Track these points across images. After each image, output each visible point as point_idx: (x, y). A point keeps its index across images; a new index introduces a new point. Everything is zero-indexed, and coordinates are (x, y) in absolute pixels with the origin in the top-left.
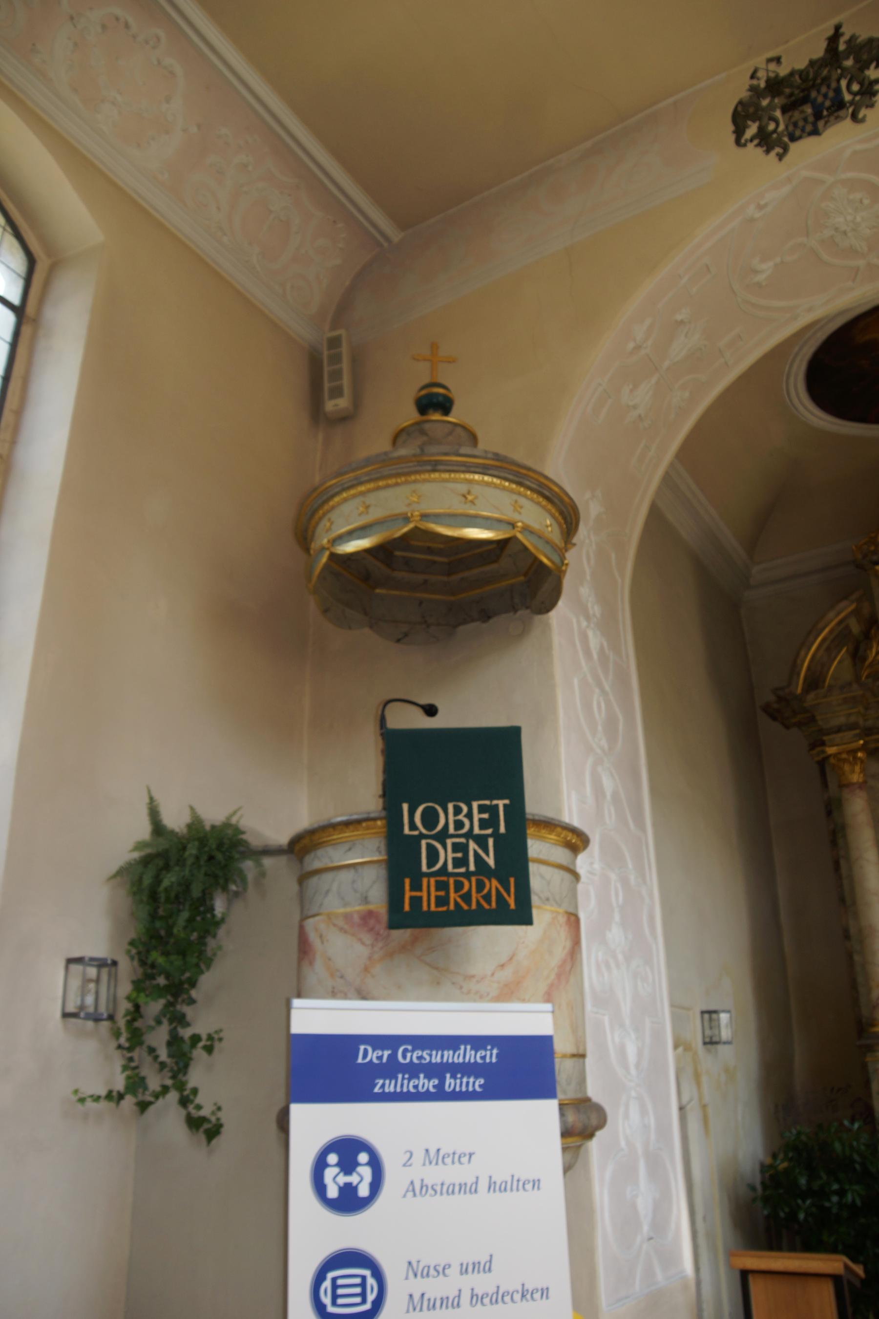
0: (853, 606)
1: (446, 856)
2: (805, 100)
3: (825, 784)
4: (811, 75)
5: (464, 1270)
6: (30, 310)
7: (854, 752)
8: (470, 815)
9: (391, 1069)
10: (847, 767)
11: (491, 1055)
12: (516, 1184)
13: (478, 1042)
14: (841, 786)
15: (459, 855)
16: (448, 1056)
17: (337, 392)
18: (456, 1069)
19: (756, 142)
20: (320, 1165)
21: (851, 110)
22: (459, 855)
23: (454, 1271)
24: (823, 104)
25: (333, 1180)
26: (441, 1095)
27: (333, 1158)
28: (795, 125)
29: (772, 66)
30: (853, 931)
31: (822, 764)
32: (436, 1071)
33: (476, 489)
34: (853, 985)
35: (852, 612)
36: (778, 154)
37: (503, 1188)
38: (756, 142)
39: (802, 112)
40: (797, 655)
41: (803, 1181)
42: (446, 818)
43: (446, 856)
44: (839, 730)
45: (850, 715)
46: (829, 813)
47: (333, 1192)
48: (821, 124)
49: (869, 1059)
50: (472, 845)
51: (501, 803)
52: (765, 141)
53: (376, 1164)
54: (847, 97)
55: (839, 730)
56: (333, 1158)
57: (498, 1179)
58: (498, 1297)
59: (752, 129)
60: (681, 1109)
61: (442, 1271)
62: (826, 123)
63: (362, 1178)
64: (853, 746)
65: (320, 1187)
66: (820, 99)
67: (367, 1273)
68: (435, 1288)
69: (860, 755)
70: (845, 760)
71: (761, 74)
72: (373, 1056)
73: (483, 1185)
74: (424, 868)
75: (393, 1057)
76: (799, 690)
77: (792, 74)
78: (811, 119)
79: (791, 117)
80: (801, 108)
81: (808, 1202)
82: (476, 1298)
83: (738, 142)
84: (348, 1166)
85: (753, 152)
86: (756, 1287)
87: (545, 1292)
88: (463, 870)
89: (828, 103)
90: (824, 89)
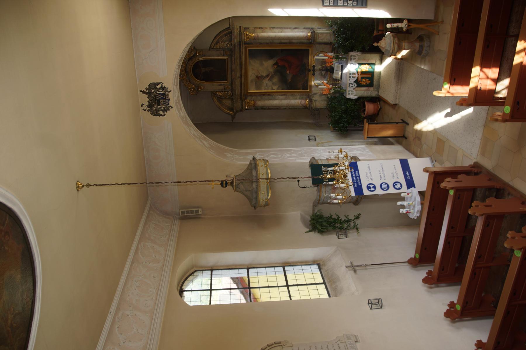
2: (159, 101)
3: (250, 109)
4: (152, 98)
5: (380, 173)
6: (210, 269)
8: (325, 172)
10: (251, 104)
11: (353, 170)
12: (369, 167)
15: (331, 173)
16: (354, 176)
17: (197, 211)
18: (356, 175)
19: (165, 112)
20: (371, 191)
21: (166, 92)
22: (331, 173)
23: (380, 174)
24: (161, 97)
25: (372, 189)
26: (359, 176)
27: (370, 189)
28: (164, 103)
29: (144, 106)
30: (285, 108)
32: (356, 177)
33: (260, 172)
34: (296, 109)
36: (171, 108)
37: (369, 168)
38: (165, 112)
39: (162, 102)
40: (225, 112)
44: (242, 105)
46: (257, 109)
47: (374, 189)
48: (167, 98)
52: (165, 110)
53: (370, 184)
54: (163, 92)
55: (242, 105)
56: (370, 189)
57: (368, 169)
58: (383, 169)
59: (161, 113)
60: (329, 146)
61: (381, 176)
62: (167, 97)
65: (373, 191)
66: (160, 98)
67: (382, 185)
68: (383, 177)
71: (145, 108)
72: (356, 185)
73: (369, 171)
75: (356, 183)
76: (233, 113)
77: (149, 102)
78: (165, 100)
79: (162, 104)
80: (160, 102)
81: (345, 124)
82: (383, 172)
83: (163, 116)
84: (370, 188)
85: (167, 113)
86: (369, 136)
87: (381, 163)
88: (333, 173)
89: (162, 96)
90: (158, 96)
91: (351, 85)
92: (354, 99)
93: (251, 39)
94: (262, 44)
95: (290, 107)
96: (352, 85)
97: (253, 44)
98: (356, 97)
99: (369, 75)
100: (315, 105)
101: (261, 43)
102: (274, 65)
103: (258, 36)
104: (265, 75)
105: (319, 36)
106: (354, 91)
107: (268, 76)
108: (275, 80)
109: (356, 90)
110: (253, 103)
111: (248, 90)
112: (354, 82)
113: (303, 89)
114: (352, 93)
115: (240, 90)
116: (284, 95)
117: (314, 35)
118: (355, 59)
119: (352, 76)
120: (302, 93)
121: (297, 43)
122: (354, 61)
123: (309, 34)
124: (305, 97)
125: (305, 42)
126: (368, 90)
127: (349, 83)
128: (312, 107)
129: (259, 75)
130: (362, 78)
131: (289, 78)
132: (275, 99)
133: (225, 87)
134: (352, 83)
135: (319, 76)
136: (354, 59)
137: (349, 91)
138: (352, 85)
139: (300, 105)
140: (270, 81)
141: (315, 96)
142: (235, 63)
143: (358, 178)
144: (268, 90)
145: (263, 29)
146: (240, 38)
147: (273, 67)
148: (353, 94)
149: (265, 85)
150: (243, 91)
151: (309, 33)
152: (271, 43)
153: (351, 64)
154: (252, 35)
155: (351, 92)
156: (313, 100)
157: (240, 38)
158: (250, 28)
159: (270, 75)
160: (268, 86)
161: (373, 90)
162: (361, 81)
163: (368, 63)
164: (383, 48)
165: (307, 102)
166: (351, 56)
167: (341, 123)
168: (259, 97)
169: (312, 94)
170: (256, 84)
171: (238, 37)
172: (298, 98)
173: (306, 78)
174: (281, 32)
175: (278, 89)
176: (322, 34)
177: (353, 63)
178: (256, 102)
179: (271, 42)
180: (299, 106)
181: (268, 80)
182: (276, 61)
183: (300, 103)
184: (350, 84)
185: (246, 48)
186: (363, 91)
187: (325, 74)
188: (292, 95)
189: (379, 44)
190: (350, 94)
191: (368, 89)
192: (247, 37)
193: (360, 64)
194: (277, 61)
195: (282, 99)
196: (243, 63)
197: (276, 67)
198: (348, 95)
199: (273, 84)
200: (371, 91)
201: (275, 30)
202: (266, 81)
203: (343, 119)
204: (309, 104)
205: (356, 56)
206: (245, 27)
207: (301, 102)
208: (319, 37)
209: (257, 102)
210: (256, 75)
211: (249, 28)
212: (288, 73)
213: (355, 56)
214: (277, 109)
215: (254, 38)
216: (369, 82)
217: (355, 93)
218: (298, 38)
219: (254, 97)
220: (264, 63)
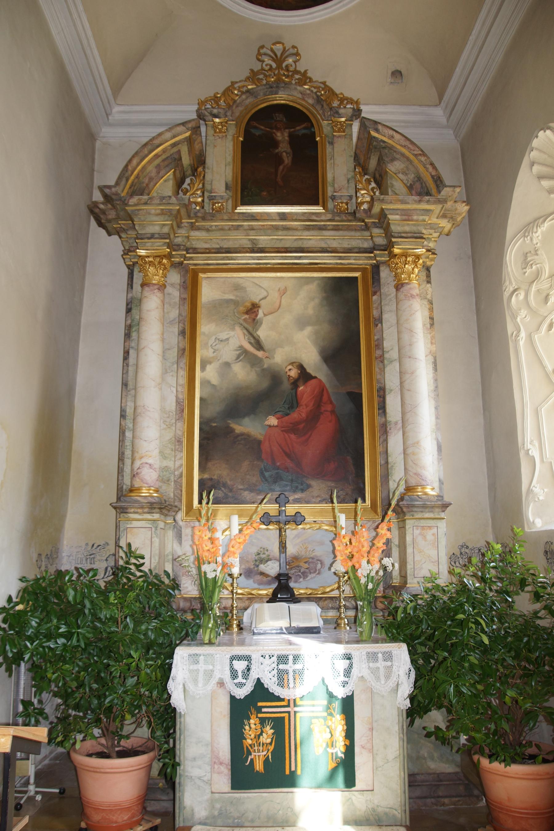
0: (188, 134)
7: (161, 257)
30: (129, 411)
31: (131, 269)
35: (186, 138)
44: (152, 236)
45: (164, 225)
46: (129, 310)
69: (165, 261)
91: (240, 666)
92: (171, 686)
95: (128, 434)
96: (240, 674)
100: (135, 524)
102: (301, 367)
104: (262, 333)
105: (430, 527)
106: (214, 681)
107: (259, 345)
109: (213, 696)
110: (156, 280)
112: (259, 684)
115: (206, 249)
118: (378, 679)
119: (290, 667)
122: (366, 673)
126: (215, 761)
127: (255, 657)
129: (260, 314)
132: (165, 371)
133: (222, 197)
134: (254, 675)
135: (254, 550)
136: (375, 672)
138: (240, 674)
139: (137, 464)
140: (238, 352)
141: (170, 534)
142: (308, 228)
145: (430, 328)
147: (292, 364)
149: (223, 336)
150: (199, 260)
151: (433, 489)
152: (381, 358)
155: (205, 671)
156: (156, 516)
158: (429, 285)
159: (260, 354)
161: (212, 793)
162: (263, 721)
163: (357, 749)
166: (388, 657)
168: (174, 313)
169: (181, 523)
170: (228, 301)
171: (407, 229)
172: (165, 463)
173: (247, 495)
175: (205, 383)
177: (355, 671)
178: (159, 289)
179: (386, 356)
181: (241, 347)
182: (313, 374)
183: (144, 460)
184: (248, 658)
185: (363, 270)
186: (207, 736)
187: (262, 574)
190: (195, 667)
191: (221, 763)
194: (315, 377)
195: (163, 399)
196: (305, 259)
197: (294, 373)
198: (190, 655)
199: (227, 365)
200: (209, 783)
204: (139, 498)
205: (391, 683)
206: (432, 270)
208: (423, 528)
209: (159, 294)
210: (263, 303)
211: (429, 282)
212: (267, 423)
213: (389, 672)
214: (125, 384)
216: (259, 766)
219: (175, 293)
220: (309, 330)
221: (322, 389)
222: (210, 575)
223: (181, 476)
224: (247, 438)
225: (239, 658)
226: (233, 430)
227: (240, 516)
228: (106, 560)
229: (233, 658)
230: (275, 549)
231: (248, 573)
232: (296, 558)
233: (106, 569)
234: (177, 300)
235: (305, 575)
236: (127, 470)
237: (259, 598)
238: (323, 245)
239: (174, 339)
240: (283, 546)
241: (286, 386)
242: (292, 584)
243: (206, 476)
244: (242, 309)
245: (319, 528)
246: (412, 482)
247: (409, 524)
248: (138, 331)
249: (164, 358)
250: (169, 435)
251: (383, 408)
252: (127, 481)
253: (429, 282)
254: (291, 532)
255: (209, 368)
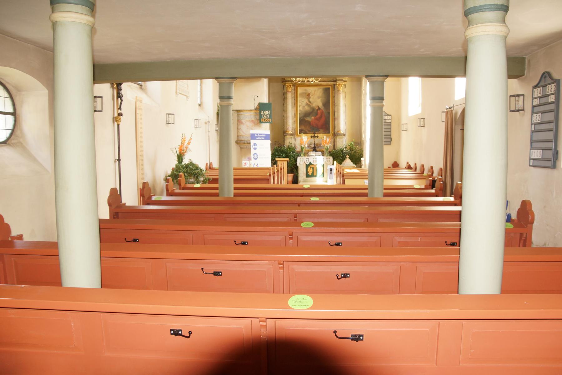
1: (265, 116)
3: (284, 89)
7: (291, 85)
9: (258, 137)
10: (289, 88)
11: (265, 136)
13: (264, 134)
14: (287, 91)
20: (253, 145)
26: (261, 139)
27: (254, 145)
30: (285, 116)
32: (261, 137)
41: (277, 154)
42: (265, 112)
43: (265, 116)
44: (288, 81)
46: (284, 95)
49: (285, 137)
50: (267, 115)
51: (270, 111)
63: (256, 147)
64: (291, 84)
70: (289, 87)
74: (263, 117)
91: (307, 160)
92: (297, 162)
93: (338, 89)
94: (334, 98)
95: (285, 121)
97: (334, 91)
98: (298, 165)
99: (315, 174)
100: (288, 138)
101: (334, 97)
102: (318, 107)
103: (340, 93)
104: (311, 100)
105: (341, 139)
106: (304, 162)
107: (310, 102)
108: (307, 108)
110: (290, 90)
111: (299, 87)
112: (310, 162)
113: (299, 130)
114: (302, 161)
116: (295, 115)
117: (341, 135)
118: (328, 161)
119: (315, 160)
120: (296, 130)
121: (334, 124)
122: (326, 161)
123: (342, 132)
124: (294, 132)
125: (335, 130)
127: (309, 159)
128: (286, 135)
129: (310, 96)
130: (313, 168)
131: (308, 119)
132: (292, 108)
135: (309, 142)
136: (327, 161)
137: (303, 158)
139: (288, 127)
143: (260, 138)
144: (299, 102)
146: (339, 80)
147: (317, 106)
148: (301, 162)
149: (303, 100)
151: (343, 131)
152: (334, 105)
153: (323, 158)
154: (341, 89)
156: (292, 136)
157: (339, 80)
159: (310, 104)
160: (302, 103)
162: (311, 168)
163: (324, 172)
164: (346, 161)
165: (290, 132)
166: (329, 158)
167: (278, 153)
168: (293, 96)
169: (296, 138)
170: (304, 93)
172: (293, 126)
173: (308, 132)
174: (343, 112)
175: (299, 110)
176: (342, 142)
179: (336, 105)
180: (287, 126)
181: (307, 103)
183: (289, 126)
185: (331, 86)
187: (311, 147)
188: (295, 122)
189: (348, 159)
192: (340, 85)
193: (323, 166)
197: (317, 108)
199: (304, 106)
201: (344, 107)
202: (306, 101)
203: (281, 154)
205: (330, 162)
206: (346, 86)
207: (290, 127)
208: (340, 139)
210: (311, 93)
211: (345, 88)
213: (329, 161)
215: (338, 91)
216: (310, 174)
217: (303, 163)
218: (339, 124)
219: (293, 91)
220: (320, 99)
221: (322, 111)
222: (303, 146)
223: (295, 128)
224: (308, 121)
225: (307, 158)
226: (305, 120)
227: (307, 136)
228: (279, 145)
229: (306, 158)
230: (313, 143)
231: (308, 147)
232: (317, 144)
233: (278, 147)
234: (294, 93)
235: (319, 147)
236: (285, 128)
237: (311, 151)
238: (323, 80)
239: (293, 101)
240: (315, 142)
241: (316, 111)
242: (316, 149)
243: (300, 128)
244: (307, 94)
245: (321, 139)
246: (339, 130)
247: (337, 138)
248: (286, 99)
249: (292, 105)
250: (293, 120)
251: (334, 115)
252: (285, 130)
253: (345, 88)
254: (316, 139)
255: (301, 107)
